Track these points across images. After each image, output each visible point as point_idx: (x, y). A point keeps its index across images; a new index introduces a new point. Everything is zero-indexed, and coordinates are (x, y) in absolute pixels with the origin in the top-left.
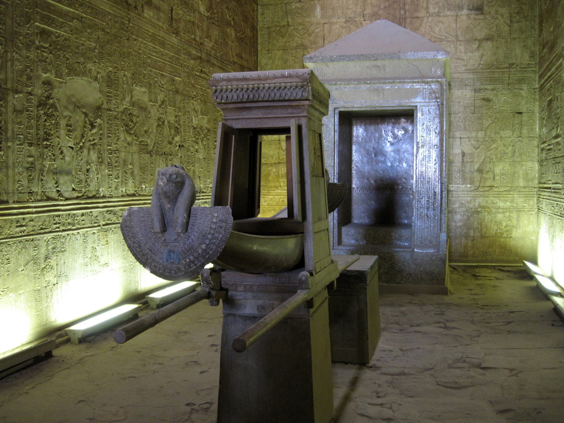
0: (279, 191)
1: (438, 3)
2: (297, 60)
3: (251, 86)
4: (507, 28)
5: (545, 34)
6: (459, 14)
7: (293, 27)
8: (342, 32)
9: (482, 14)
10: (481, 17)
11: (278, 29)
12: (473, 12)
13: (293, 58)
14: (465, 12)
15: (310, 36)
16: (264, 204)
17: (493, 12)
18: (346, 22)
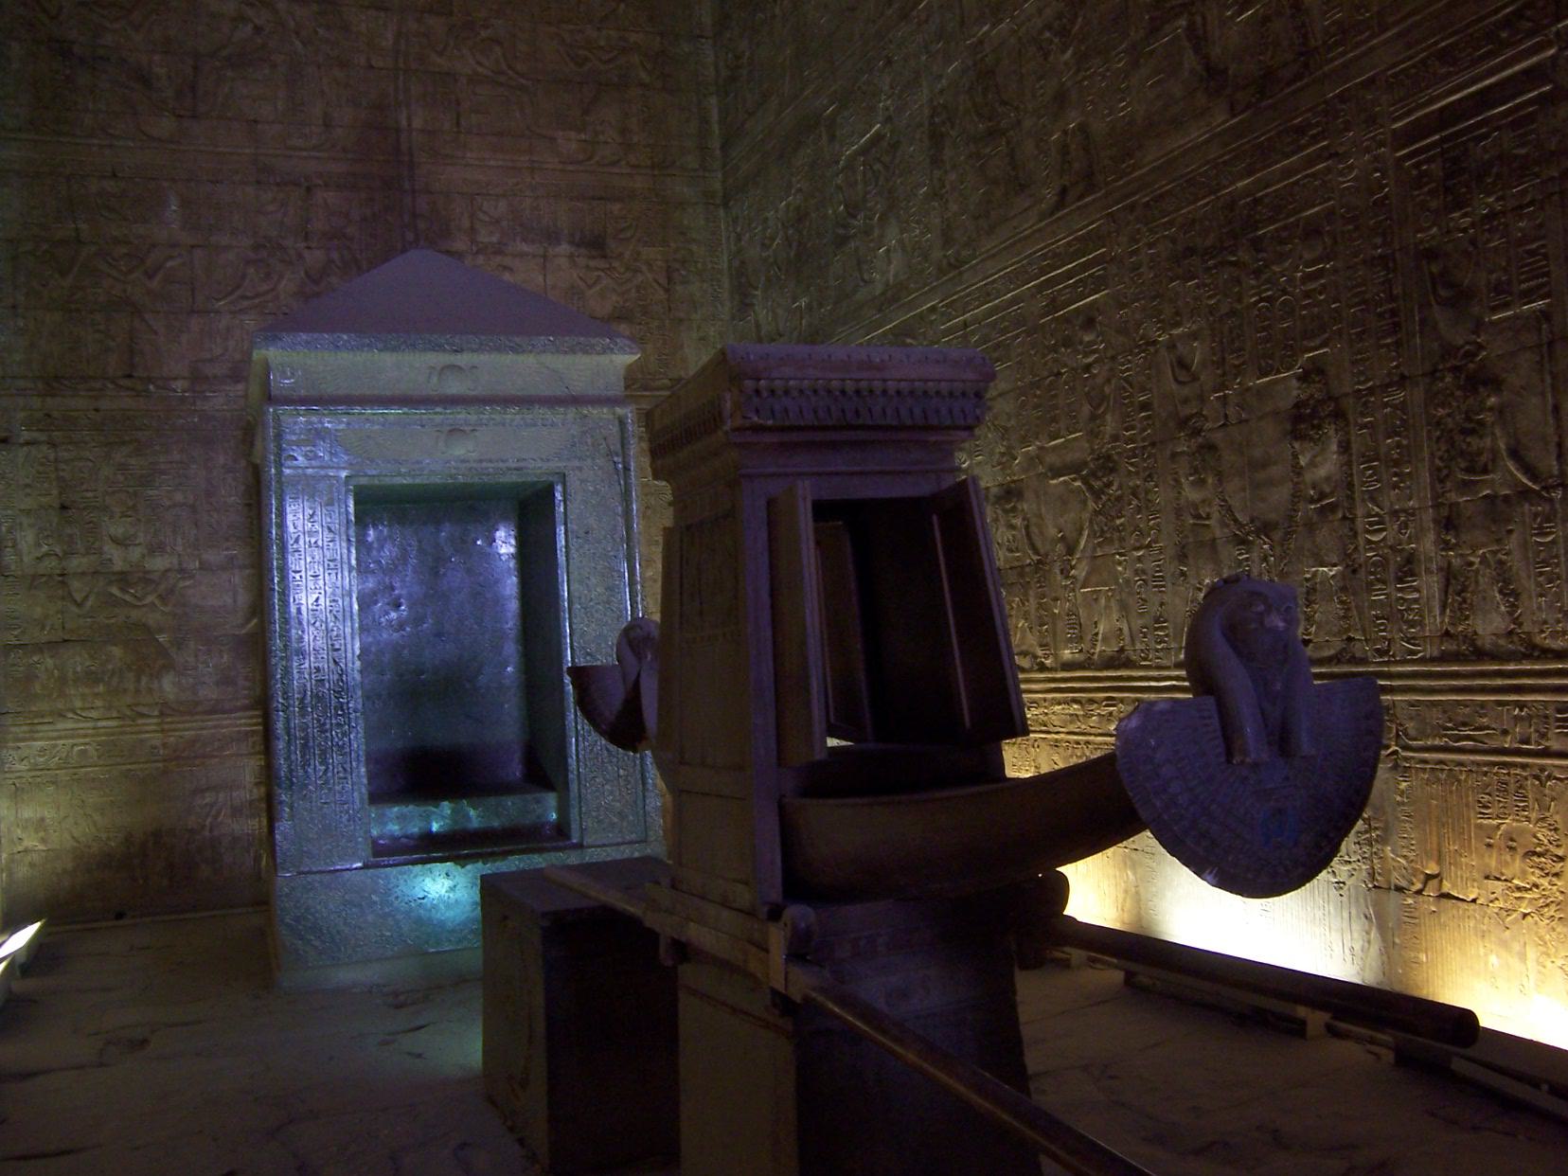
0: (70, 725)
1: (498, 222)
2: (112, 344)
3: (850, 386)
4: (661, 295)
5: (761, 313)
6: (551, 252)
7: (93, 249)
8: (244, 277)
9: (605, 257)
10: (602, 264)
11: (45, 247)
12: (583, 251)
13: (97, 336)
14: (564, 248)
15: (151, 277)
16: (18, 767)
17: (627, 254)
18: (257, 247)
